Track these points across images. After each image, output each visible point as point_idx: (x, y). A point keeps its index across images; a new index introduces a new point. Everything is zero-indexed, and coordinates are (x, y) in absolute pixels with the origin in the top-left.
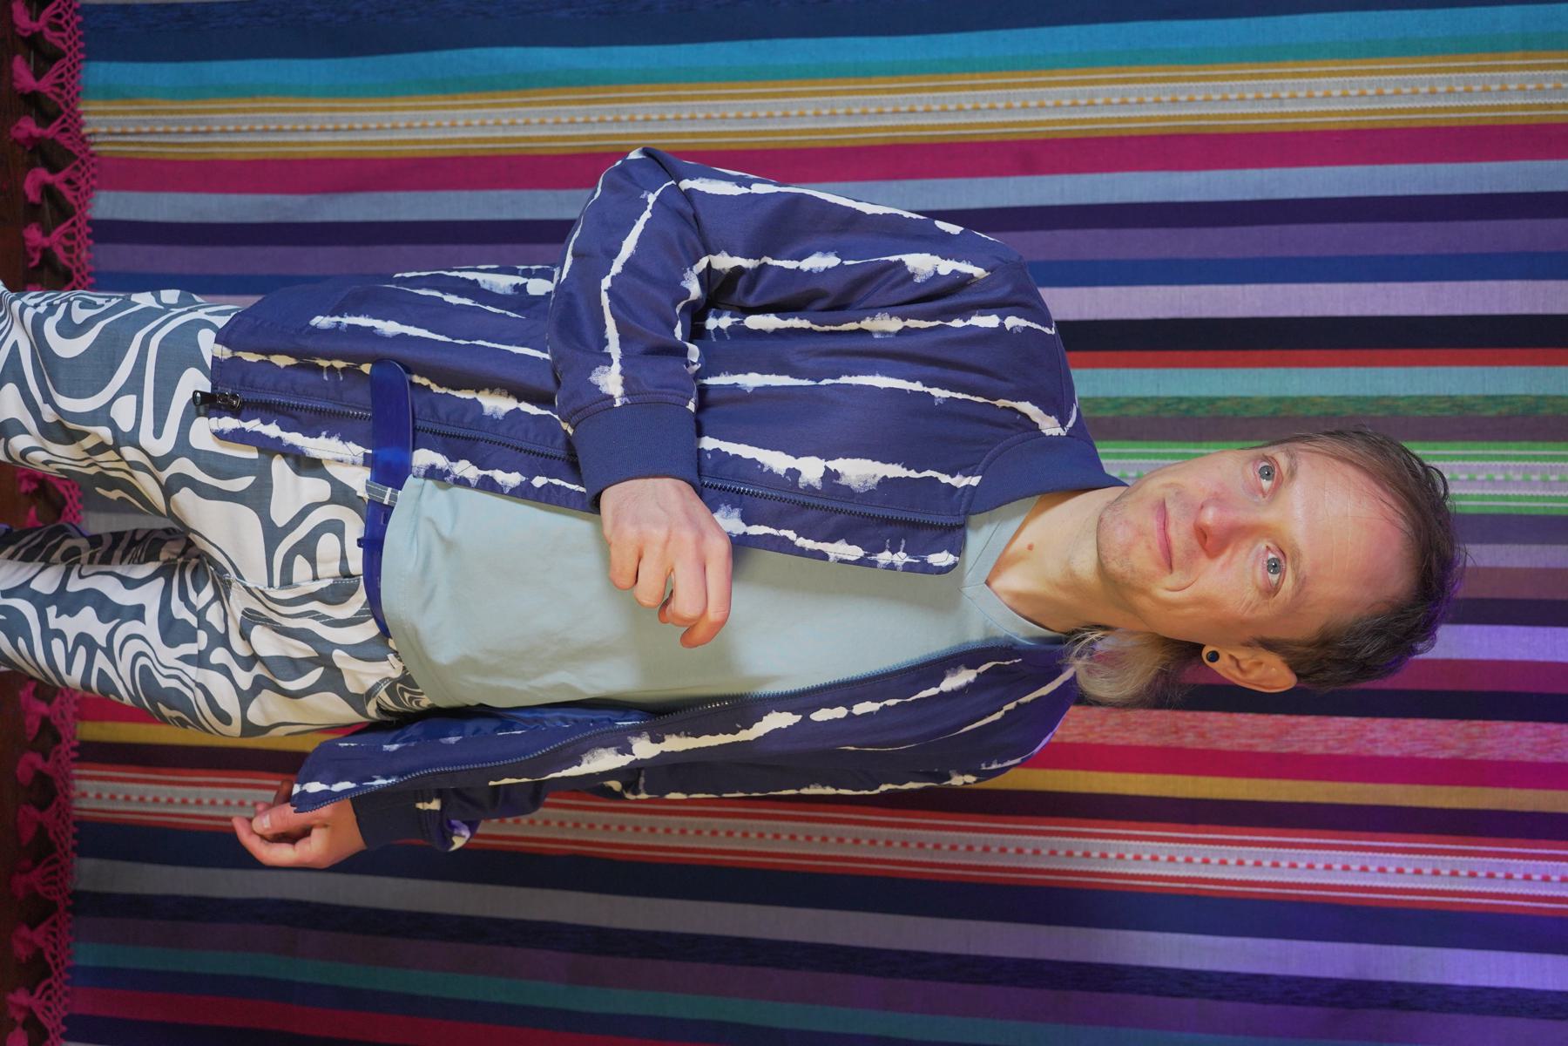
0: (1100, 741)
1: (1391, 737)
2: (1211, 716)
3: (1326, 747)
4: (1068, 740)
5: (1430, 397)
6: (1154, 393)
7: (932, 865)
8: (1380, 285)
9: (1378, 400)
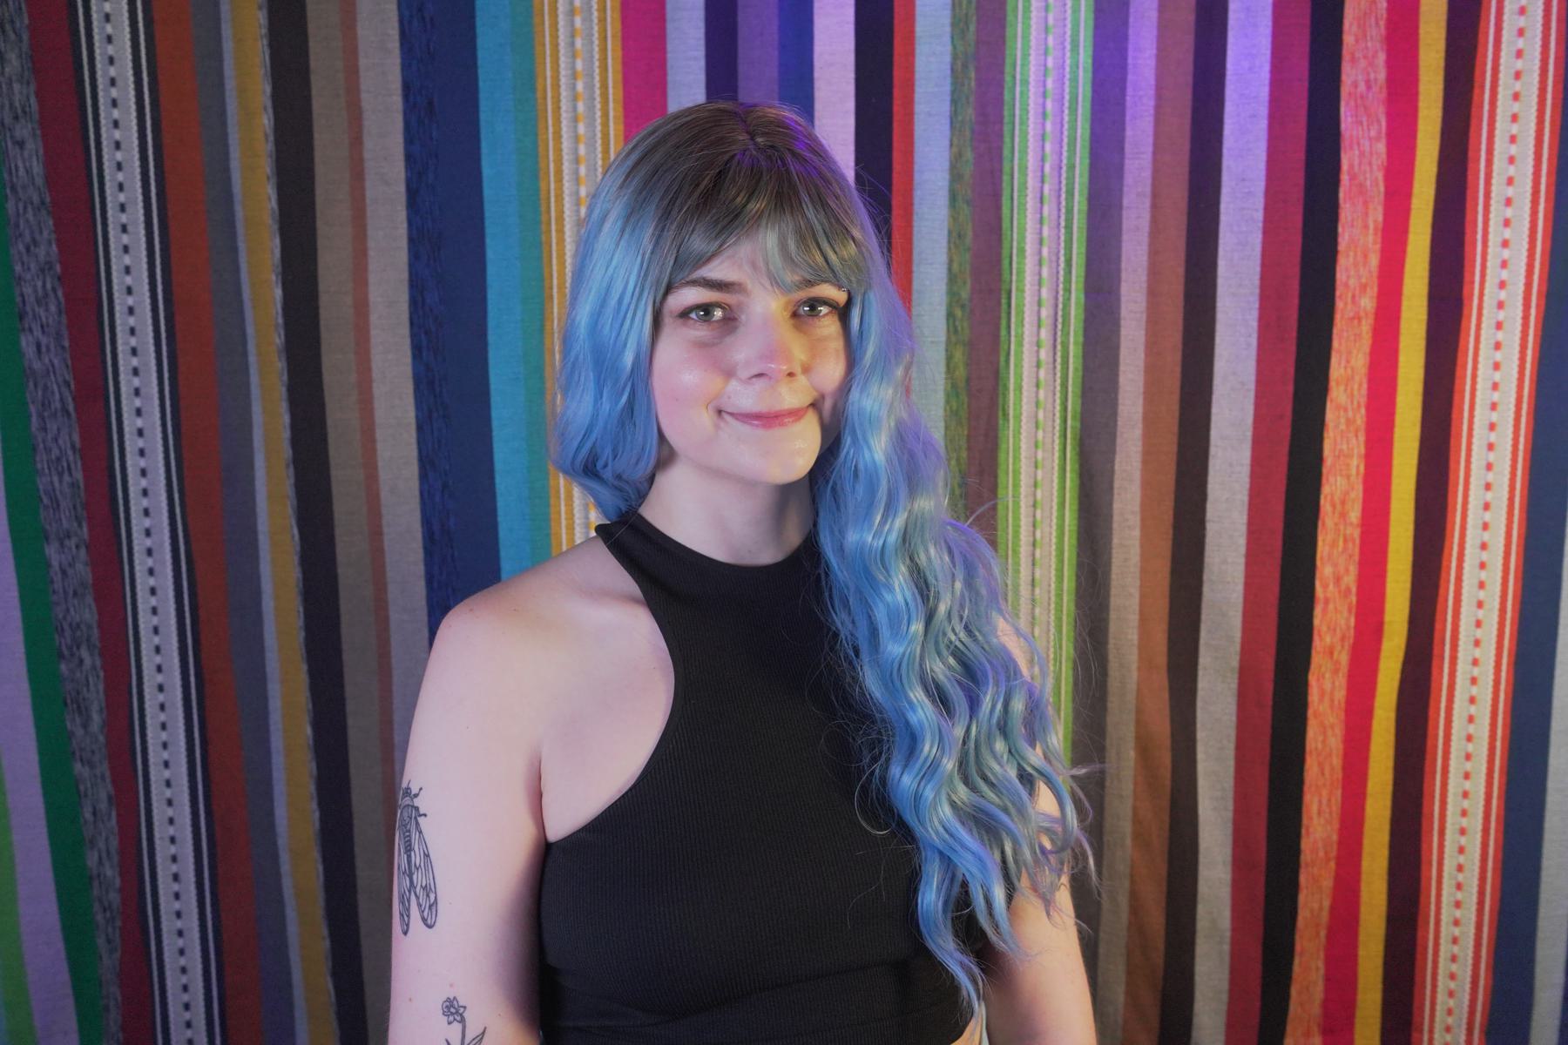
0: (1363, 411)
1: (1363, 63)
2: (1341, 276)
3: (1378, 139)
4: (1363, 450)
5: (954, 16)
6: (942, 347)
7: (1503, 610)
8: (817, 74)
9: (957, 75)
